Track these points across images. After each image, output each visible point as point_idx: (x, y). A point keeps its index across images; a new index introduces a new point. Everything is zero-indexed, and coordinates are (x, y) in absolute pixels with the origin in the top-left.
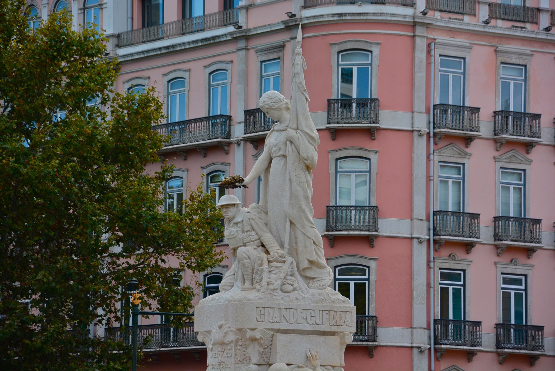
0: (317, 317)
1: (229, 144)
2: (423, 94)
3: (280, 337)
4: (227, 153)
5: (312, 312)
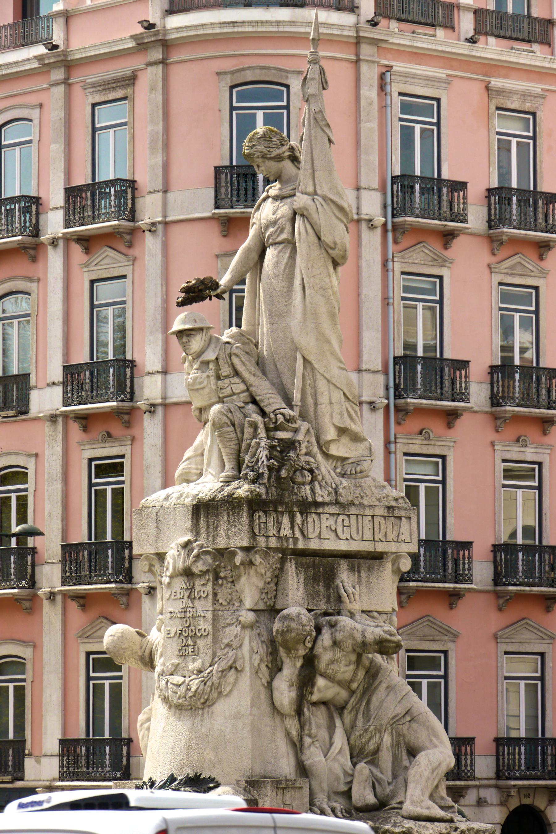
0: (354, 528)
1: (133, 232)
2: (374, 158)
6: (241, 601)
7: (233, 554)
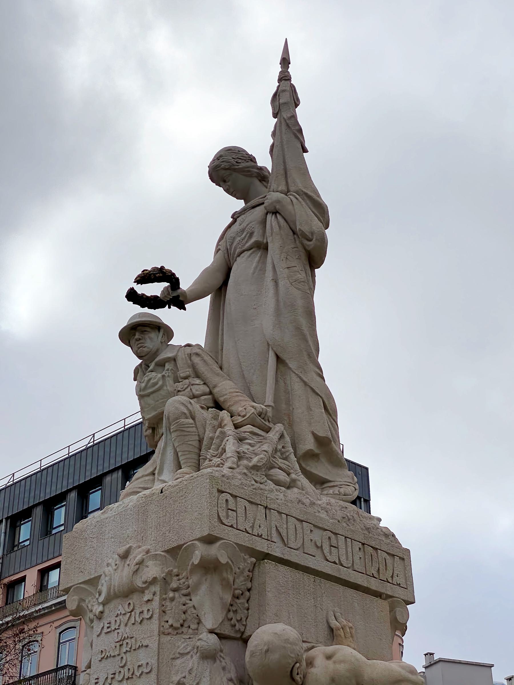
0: (342, 551)
5: (333, 536)
6: (199, 622)
7: (190, 549)
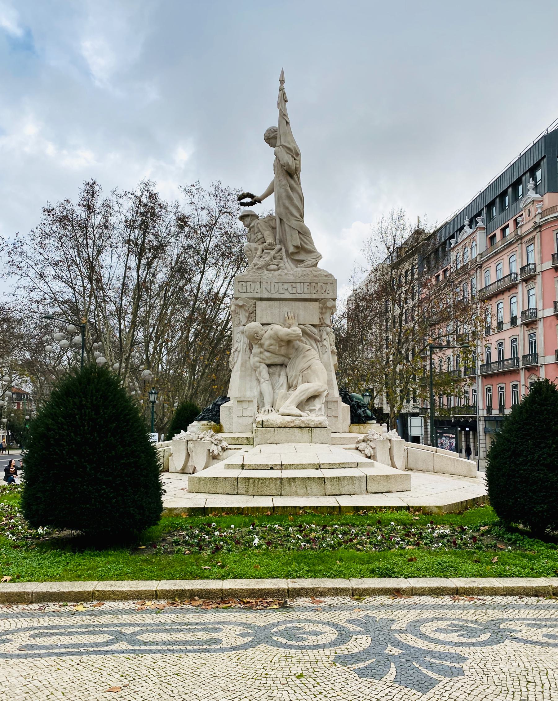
3: (259, 303)
4: (517, 288)
